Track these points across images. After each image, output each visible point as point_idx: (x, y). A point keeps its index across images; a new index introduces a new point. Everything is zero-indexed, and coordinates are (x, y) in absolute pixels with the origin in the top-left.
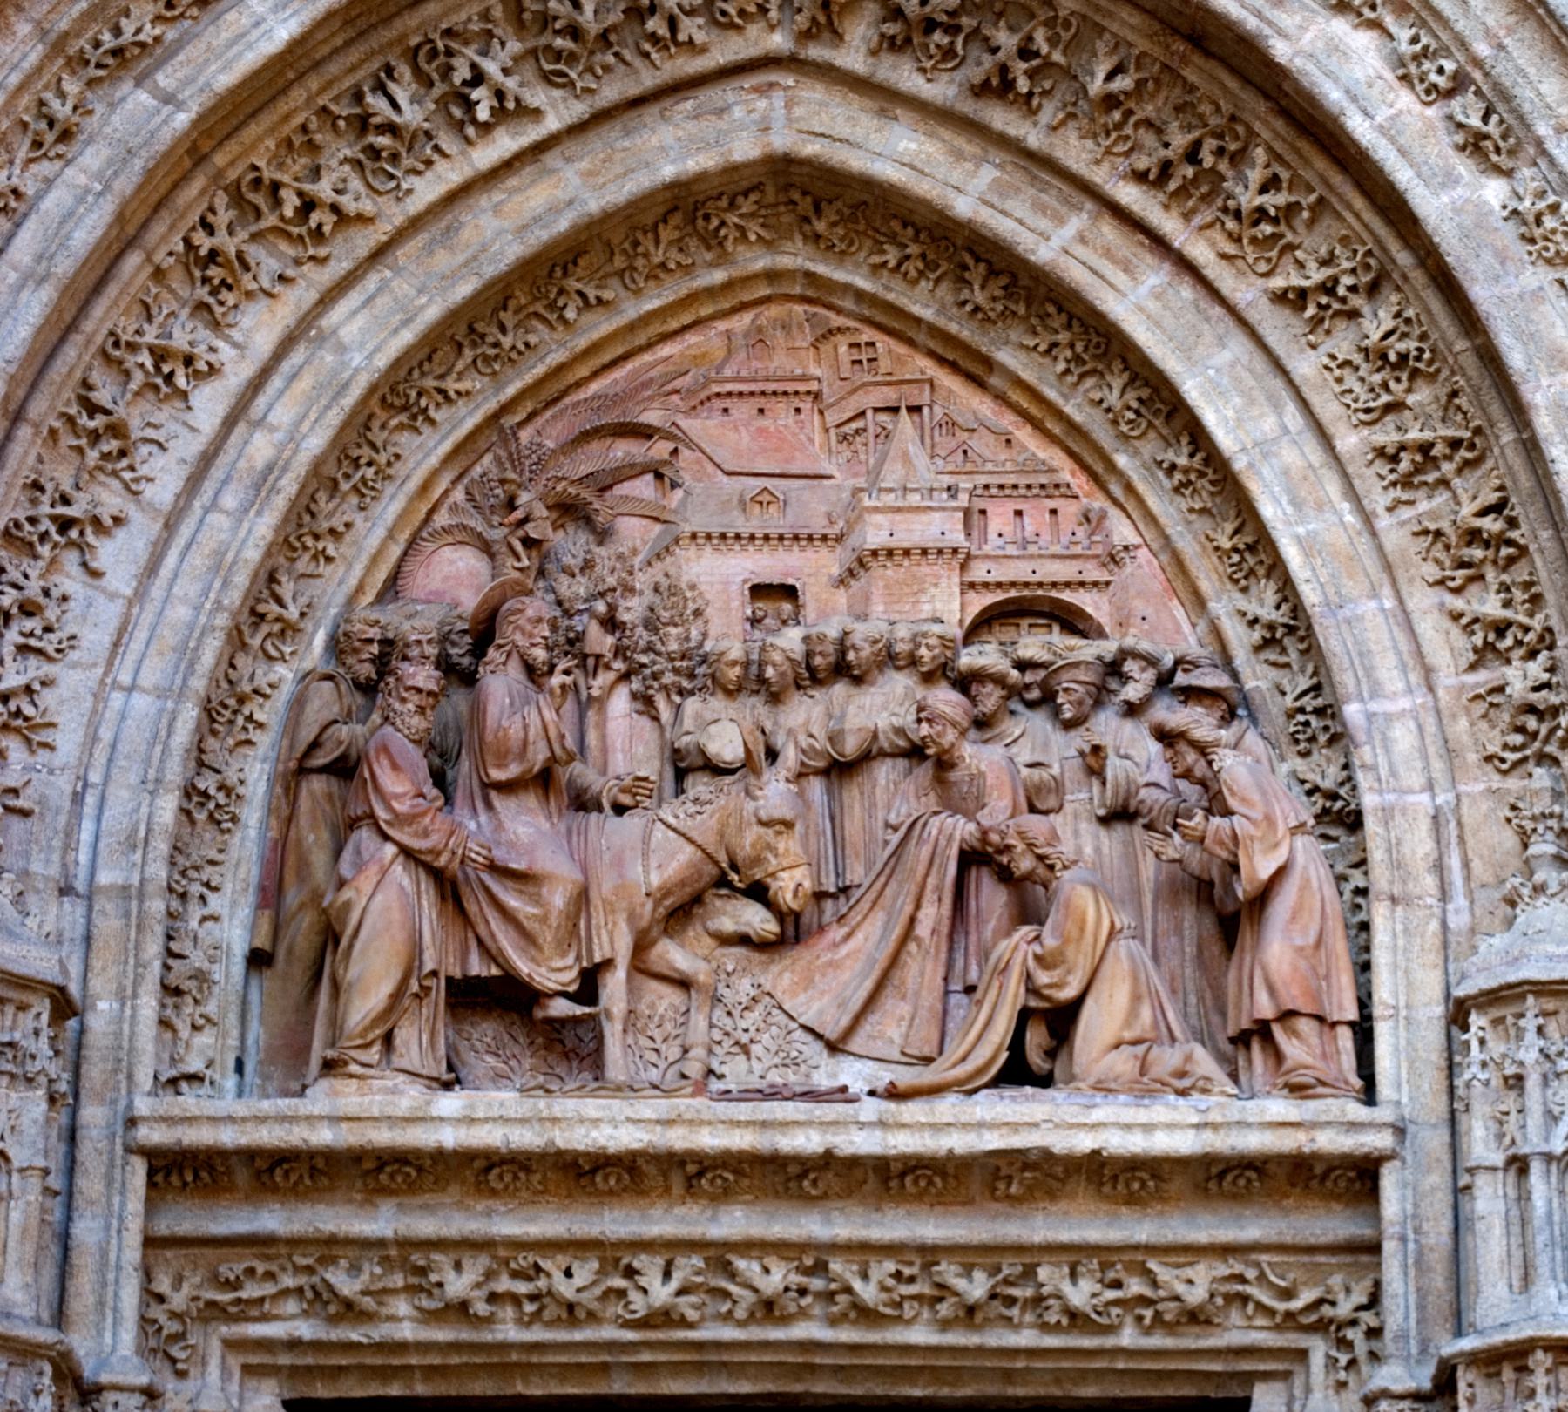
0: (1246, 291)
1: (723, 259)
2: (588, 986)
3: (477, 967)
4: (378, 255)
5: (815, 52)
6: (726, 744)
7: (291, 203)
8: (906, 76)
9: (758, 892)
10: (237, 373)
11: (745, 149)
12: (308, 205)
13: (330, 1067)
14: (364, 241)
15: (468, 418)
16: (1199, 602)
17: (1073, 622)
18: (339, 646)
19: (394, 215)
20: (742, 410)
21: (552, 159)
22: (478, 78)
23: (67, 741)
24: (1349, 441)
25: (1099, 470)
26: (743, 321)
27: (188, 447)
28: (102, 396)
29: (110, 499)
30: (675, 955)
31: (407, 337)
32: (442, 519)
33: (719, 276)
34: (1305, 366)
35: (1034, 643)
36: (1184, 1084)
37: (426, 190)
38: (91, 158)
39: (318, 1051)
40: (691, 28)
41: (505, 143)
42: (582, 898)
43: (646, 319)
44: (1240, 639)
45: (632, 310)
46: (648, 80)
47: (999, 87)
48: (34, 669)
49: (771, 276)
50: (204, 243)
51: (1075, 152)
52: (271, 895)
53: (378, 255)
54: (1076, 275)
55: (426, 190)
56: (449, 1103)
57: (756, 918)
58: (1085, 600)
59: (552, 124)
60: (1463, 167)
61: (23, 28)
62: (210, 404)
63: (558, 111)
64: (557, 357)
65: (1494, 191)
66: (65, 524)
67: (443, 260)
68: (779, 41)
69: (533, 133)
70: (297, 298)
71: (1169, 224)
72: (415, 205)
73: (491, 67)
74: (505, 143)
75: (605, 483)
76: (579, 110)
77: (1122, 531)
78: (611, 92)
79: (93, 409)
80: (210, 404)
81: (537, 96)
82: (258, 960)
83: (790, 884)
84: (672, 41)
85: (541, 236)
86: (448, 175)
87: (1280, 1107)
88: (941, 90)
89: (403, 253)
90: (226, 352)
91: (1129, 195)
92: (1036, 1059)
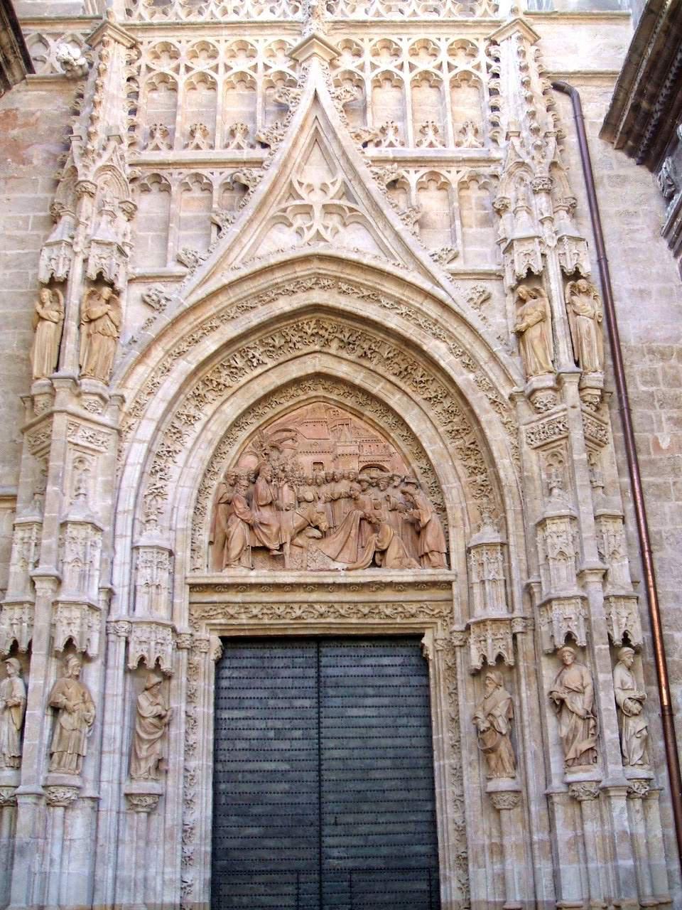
0: (418, 398)
2: (281, 546)
3: (258, 544)
5: (325, 350)
6: (309, 496)
7: (215, 383)
8: (344, 354)
9: (317, 527)
10: (204, 419)
12: (219, 384)
13: (227, 565)
14: (230, 391)
15: (251, 428)
16: (409, 464)
17: (382, 469)
18: (226, 477)
19: (236, 386)
20: (311, 425)
21: (269, 373)
22: (254, 357)
23: (170, 497)
24: (441, 429)
25: (387, 436)
27: (194, 435)
29: (178, 447)
30: (299, 541)
31: (240, 411)
32: (247, 450)
33: (305, 397)
34: (431, 414)
35: (375, 473)
36: (409, 566)
37: (243, 380)
39: (225, 562)
41: (259, 370)
42: (280, 529)
44: (418, 471)
45: (287, 405)
46: (290, 357)
49: (316, 397)
50: (197, 393)
51: (381, 369)
52: (213, 530)
54: (381, 395)
55: (243, 380)
56: (253, 573)
57: (317, 533)
58: (386, 465)
59: (269, 366)
60: (465, 371)
61: (160, 349)
62: (198, 426)
64: (270, 415)
65: (471, 376)
66: (169, 452)
67: (248, 395)
68: (317, 348)
69: (266, 368)
70: (217, 403)
71: (401, 384)
73: (257, 355)
74: (259, 370)
76: (275, 363)
77: (392, 449)
78: (282, 359)
81: (266, 360)
82: (211, 543)
83: (323, 526)
84: (294, 347)
86: (248, 377)
87: (430, 571)
88: (352, 357)
89: (238, 393)
90: (202, 416)
91: (393, 378)
92: (377, 561)
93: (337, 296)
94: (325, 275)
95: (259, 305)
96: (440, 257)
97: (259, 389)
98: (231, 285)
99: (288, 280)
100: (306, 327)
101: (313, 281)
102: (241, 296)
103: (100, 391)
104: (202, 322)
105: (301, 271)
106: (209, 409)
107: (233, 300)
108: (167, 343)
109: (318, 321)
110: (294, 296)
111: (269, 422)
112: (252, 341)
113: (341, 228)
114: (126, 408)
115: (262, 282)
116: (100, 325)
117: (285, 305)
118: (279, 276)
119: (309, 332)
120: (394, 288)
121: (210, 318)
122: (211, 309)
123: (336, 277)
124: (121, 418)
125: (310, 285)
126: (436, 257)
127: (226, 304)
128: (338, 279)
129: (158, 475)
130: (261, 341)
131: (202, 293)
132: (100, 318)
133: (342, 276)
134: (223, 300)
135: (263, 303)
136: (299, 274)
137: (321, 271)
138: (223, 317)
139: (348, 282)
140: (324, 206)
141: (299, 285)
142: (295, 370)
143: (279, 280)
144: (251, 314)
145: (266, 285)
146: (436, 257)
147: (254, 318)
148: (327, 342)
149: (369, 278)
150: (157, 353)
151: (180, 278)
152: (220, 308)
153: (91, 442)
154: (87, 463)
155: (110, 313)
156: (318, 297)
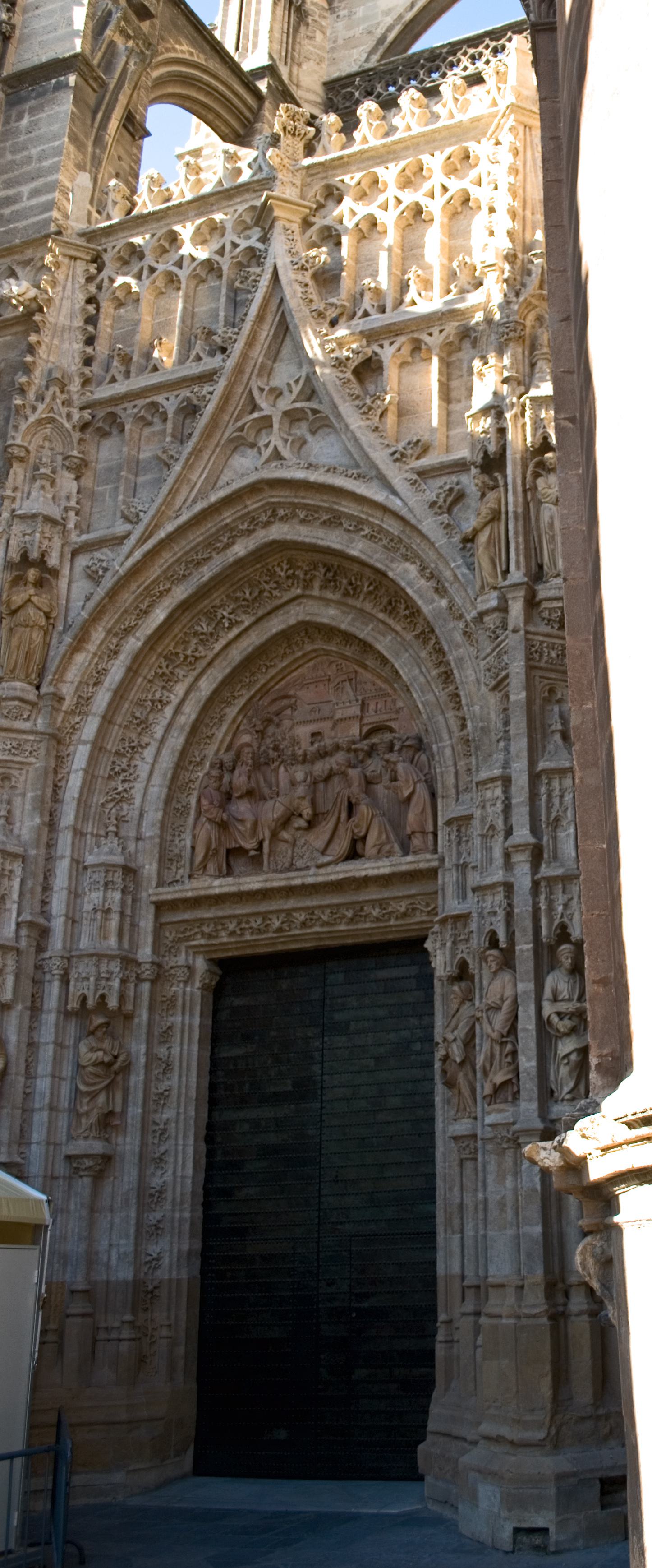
1: (301, 649)
4: (209, 664)
5: (308, 592)
7: (182, 657)
8: (329, 595)
11: (292, 621)
12: (186, 657)
15: (242, 702)
19: (211, 655)
20: (312, 687)
21: (250, 632)
22: (223, 617)
23: (138, 802)
26: (312, 663)
27: (165, 722)
28: (138, 714)
31: (214, 685)
32: (242, 728)
33: (300, 654)
38: (122, 657)
40: (276, 593)
41: (235, 631)
43: (285, 667)
45: (281, 666)
46: (269, 608)
47: (346, 594)
48: (126, 785)
49: (315, 651)
50: (160, 671)
53: (209, 664)
59: (247, 624)
61: (100, 629)
62: (169, 711)
63: (247, 620)
64: (262, 682)
66: (133, 748)
67: (225, 664)
68: (299, 591)
69: (242, 627)
72: (216, 651)
73: (225, 613)
74: (235, 631)
75: (278, 714)
76: (253, 619)
78: (260, 613)
79: (136, 718)
80: (169, 711)
84: (271, 597)
85: (245, 653)
86: (223, 642)
89: (216, 663)
93: (298, 527)
94: (279, 503)
95: (214, 554)
96: (403, 455)
97: (236, 655)
98: (171, 538)
99: (239, 518)
100: (278, 569)
101: (269, 513)
102: (188, 548)
103: (18, 694)
104: (146, 588)
105: (252, 504)
106: (180, 689)
107: (179, 555)
108: (108, 621)
109: (289, 561)
110: (253, 536)
111: (264, 691)
112: (216, 598)
113: (309, 438)
114: (66, 705)
115: (210, 527)
116: (21, 616)
117: (240, 549)
118: (228, 516)
119: (282, 574)
120: (351, 505)
121: (156, 581)
122: (155, 571)
123: (290, 503)
124: (60, 719)
125: (265, 519)
126: (397, 455)
127: (170, 561)
128: (295, 506)
129: (121, 778)
130: (228, 596)
131: (138, 554)
132: (19, 608)
133: (296, 501)
134: (167, 557)
135: (220, 551)
136: (250, 508)
137: (273, 500)
138: (173, 577)
139: (305, 507)
140: (286, 413)
141: (254, 523)
142: (276, 625)
143: (228, 521)
144: (205, 569)
145: (214, 530)
146: (397, 455)
147: (206, 573)
148: (307, 585)
149: (325, 497)
150: (98, 635)
151: (120, 540)
152: (165, 567)
153: (14, 754)
154: (13, 779)
155: (35, 599)
156: (278, 532)
